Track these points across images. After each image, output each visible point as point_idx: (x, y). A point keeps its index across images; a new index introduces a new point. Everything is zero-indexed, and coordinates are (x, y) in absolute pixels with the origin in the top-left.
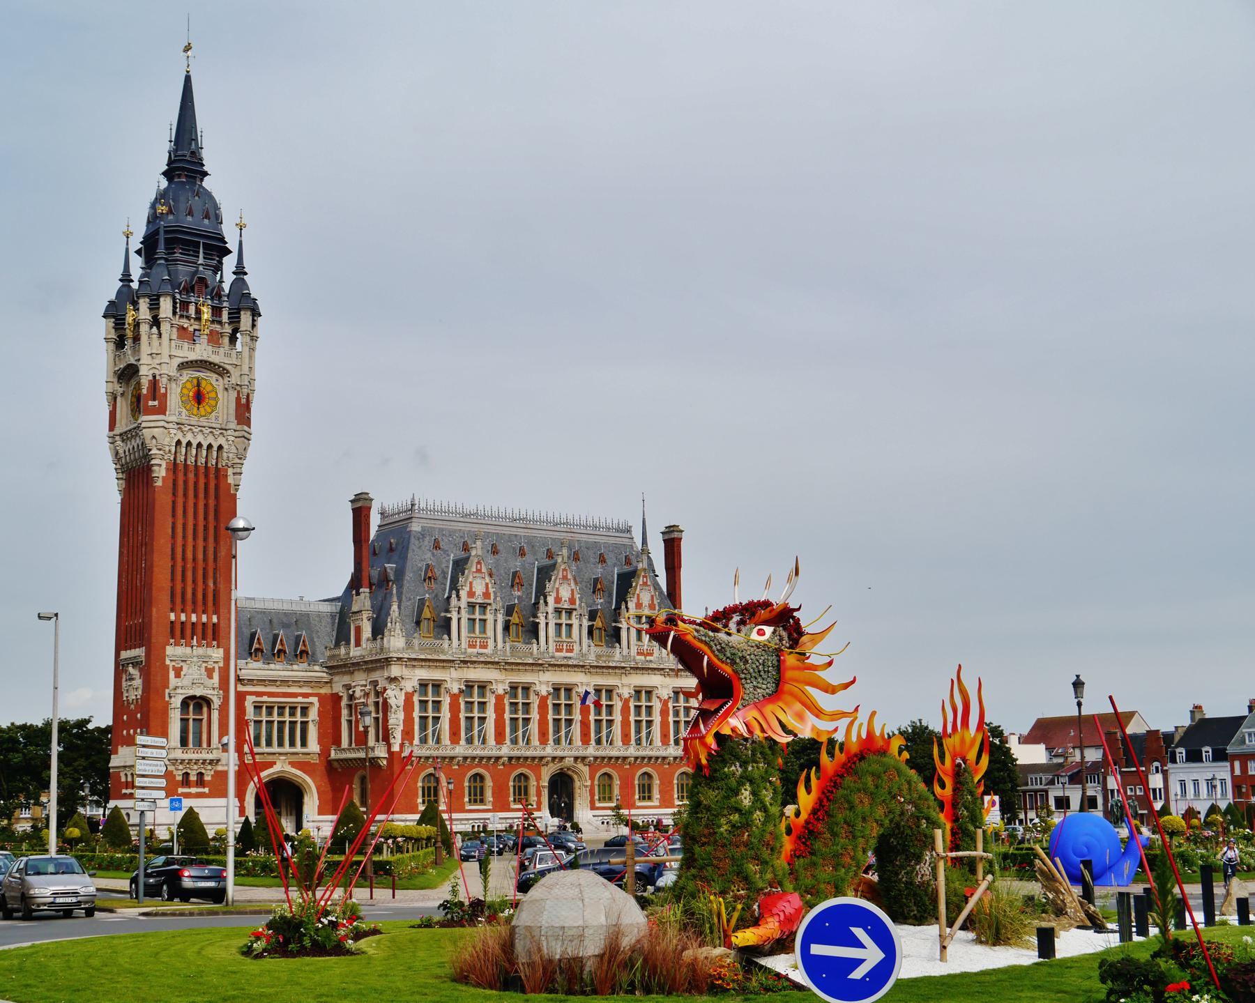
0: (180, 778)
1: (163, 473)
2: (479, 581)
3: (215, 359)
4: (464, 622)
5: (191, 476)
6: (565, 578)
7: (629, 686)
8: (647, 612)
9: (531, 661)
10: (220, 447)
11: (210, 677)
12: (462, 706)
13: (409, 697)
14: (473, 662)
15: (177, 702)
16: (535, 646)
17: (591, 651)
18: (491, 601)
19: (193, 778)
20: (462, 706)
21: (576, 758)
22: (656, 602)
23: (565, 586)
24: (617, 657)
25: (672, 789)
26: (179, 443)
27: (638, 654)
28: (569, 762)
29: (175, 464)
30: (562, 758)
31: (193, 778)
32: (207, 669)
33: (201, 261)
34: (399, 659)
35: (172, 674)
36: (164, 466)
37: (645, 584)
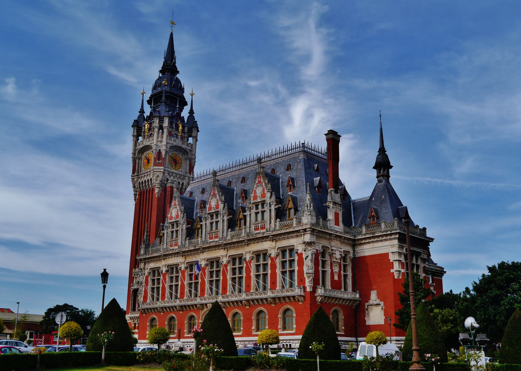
3: (149, 144)
5: (145, 195)
8: (259, 200)
9: (192, 248)
10: (151, 179)
13: (147, 278)
16: (200, 238)
17: (229, 236)
20: (168, 279)
22: (266, 191)
23: (214, 199)
24: (243, 235)
27: (256, 229)
29: (141, 192)
30: (206, 304)
34: (141, 259)
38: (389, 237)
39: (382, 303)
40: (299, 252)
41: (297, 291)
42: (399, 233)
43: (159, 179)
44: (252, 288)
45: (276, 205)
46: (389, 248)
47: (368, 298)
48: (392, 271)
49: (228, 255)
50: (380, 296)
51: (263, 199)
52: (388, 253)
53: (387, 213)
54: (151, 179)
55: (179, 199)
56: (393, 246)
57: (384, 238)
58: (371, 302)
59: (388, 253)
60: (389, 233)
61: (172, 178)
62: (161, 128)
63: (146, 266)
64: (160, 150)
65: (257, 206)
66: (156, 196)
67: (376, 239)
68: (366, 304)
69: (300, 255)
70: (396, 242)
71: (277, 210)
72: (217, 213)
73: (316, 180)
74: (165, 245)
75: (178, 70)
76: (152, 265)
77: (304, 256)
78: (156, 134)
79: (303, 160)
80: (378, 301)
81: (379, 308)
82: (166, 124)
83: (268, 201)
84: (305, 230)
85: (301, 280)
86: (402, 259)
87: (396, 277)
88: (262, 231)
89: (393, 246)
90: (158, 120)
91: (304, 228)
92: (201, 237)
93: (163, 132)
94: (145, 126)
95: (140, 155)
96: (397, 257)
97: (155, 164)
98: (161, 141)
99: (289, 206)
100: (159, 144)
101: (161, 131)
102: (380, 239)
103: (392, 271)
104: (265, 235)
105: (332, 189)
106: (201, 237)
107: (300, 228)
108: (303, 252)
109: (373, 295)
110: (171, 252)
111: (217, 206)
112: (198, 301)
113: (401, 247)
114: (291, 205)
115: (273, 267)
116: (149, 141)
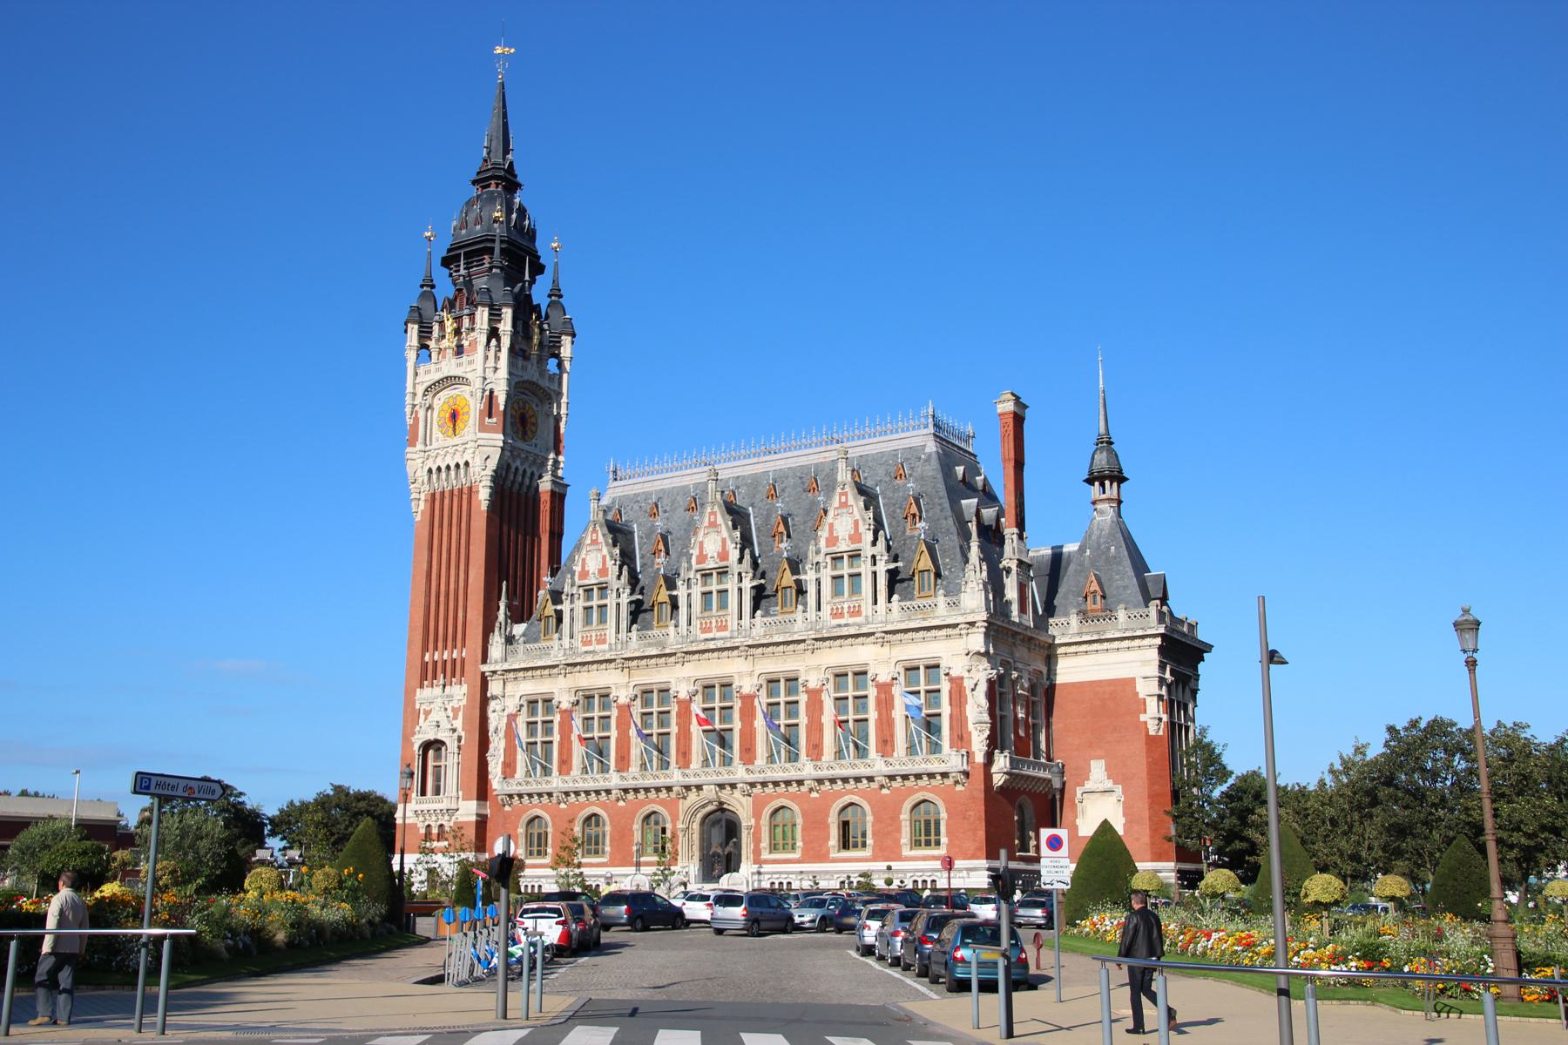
0: (423, 831)
1: (422, 506)
2: (593, 554)
3: (458, 372)
4: (579, 613)
5: (447, 502)
6: (713, 525)
7: (818, 667)
8: (843, 546)
9: (654, 652)
10: (467, 464)
11: (455, 718)
12: (577, 723)
13: (512, 718)
14: (583, 664)
15: (416, 747)
16: (671, 630)
18: (608, 579)
19: (435, 831)
20: (577, 723)
21: (721, 786)
22: (862, 528)
23: (713, 536)
24: (799, 625)
25: (898, 830)
26: (430, 471)
28: (709, 792)
29: (433, 495)
30: (699, 787)
31: (435, 831)
32: (453, 709)
33: (463, 272)
34: (494, 672)
35: (422, 717)
36: (423, 497)
37: (844, 505)
38: (1137, 642)
39: (1119, 789)
40: (954, 673)
41: (952, 760)
42: (1162, 635)
43: (493, 464)
44: (826, 750)
45: (887, 562)
46: (1140, 665)
47: (1084, 776)
48: (1143, 718)
49: (757, 673)
50: (1111, 773)
51: (853, 547)
52: (1133, 680)
53: (1125, 588)
54: (467, 464)
55: (605, 530)
56: (1145, 662)
57: (1126, 643)
58: (1089, 786)
59: (1133, 680)
60: (1139, 633)
61: (518, 463)
62: (493, 333)
63: (509, 686)
64: (491, 392)
65: (837, 559)
66: (484, 506)
67: (1106, 645)
68: (1079, 791)
69: (957, 682)
70: (1154, 655)
71: (893, 576)
72: (723, 573)
73: (969, 506)
74: (566, 641)
75: (519, 179)
76: (530, 687)
77: (968, 684)
78: (481, 348)
79: (934, 456)
80: (1109, 784)
81: (1112, 799)
82: (506, 326)
83: (868, 551)
84: (972, 624)
85: (961, 738)
86: (1164, 691)
87: (1152, 733)
88: (851, 621)
89: (1145, 662)
90: (486, 314)
91: (970, 619)
92: (676, 626)
93: (499, 346)
94: (441, 323)
95: (429, 397)
96: (1153, 687)
97: (483, 428)
98: (496, 369)
99: (921, 566)
100: (489, 374)
101: (494, 342)
102: (1116, 644)
103: (1143, 718)
104: (864, 630)
105: (1015, 530)
106: (676, 626)
107: (959, 620)
108: (966, 675)
109: (1098, 769)
110: (589, 658)
111: (723, 555)
112: (675, 776)
113: (1162, 667)
114: (925, 562)
115: (886, 703)
116: (459, 365)
